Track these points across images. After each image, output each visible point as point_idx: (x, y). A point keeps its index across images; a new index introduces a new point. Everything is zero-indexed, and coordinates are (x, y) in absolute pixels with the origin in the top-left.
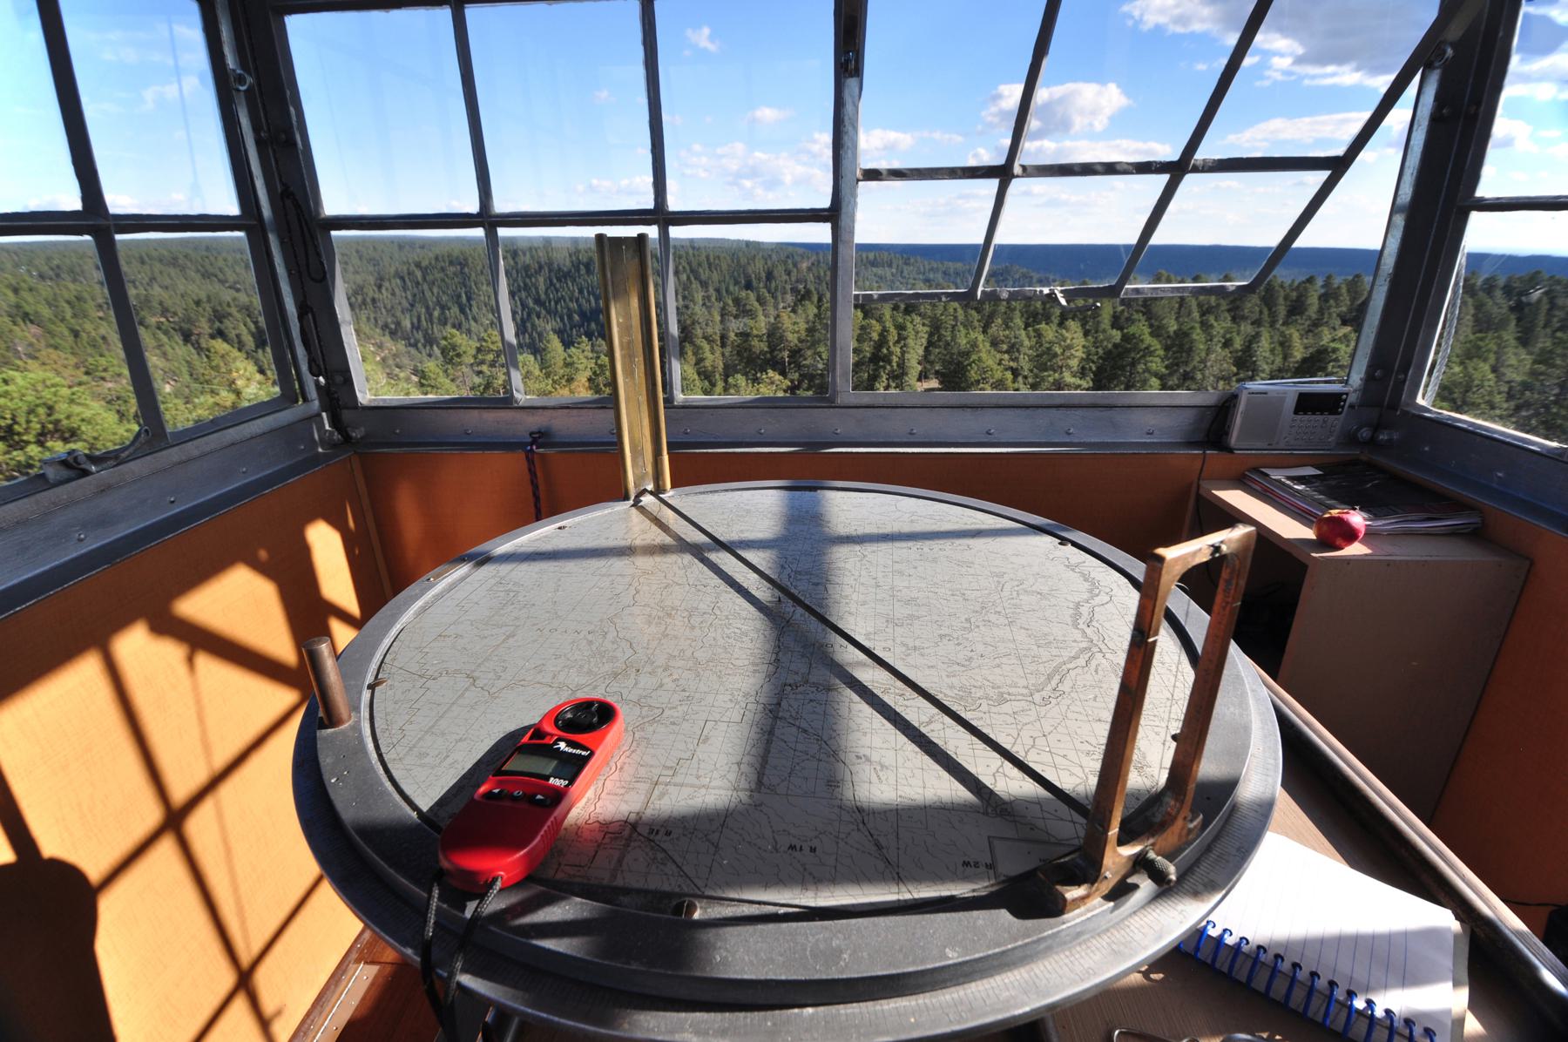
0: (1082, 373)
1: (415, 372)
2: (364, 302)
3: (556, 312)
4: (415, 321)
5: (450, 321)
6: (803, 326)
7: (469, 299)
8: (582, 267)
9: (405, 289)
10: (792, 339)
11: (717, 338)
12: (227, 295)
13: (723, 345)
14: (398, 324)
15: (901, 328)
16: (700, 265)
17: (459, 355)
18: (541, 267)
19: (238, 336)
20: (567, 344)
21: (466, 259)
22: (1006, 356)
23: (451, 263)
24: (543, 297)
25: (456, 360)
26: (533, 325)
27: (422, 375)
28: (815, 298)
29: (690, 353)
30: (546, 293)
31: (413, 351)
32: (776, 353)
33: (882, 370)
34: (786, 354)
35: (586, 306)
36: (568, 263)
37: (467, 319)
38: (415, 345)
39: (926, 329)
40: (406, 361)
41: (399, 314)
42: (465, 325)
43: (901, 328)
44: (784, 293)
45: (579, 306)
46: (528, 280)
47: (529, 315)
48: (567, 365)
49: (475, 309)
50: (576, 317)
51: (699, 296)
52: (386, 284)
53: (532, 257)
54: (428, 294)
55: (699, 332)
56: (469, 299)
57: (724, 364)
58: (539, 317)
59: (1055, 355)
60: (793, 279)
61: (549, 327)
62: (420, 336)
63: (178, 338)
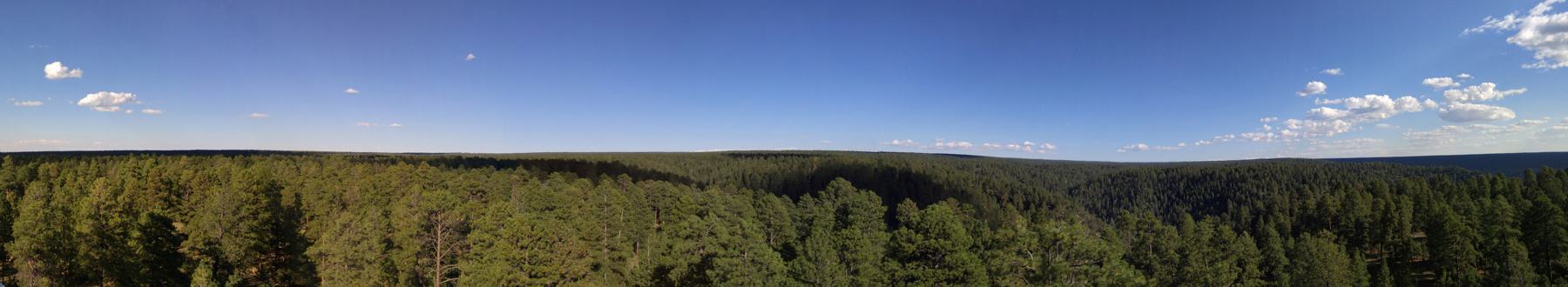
0: (1514, 225)
1: (1099, 231)
2: (1079, 193)
3: (1189, 202)
4: (1104, 204)
5: (1123, 206)
6: (1339, 203)
7: (1135, 194)
8: (1208, 177)
9: (1101, 187)
10: (1333, 210)
11: (1287, 211)
12: (1018, 184)
13: (1291, 215)
14: (1094, 205)
15: (1397, 202)
16: (1276, 172)
17: (1127, 224)
18: (1182, 178)
19: (1018, 203)
20: (1197, 219)
21: (1137, 174)
22: (1464, 217)
23: (1128, 176)
24: (1182, 192)
25: (1125, 226)
26: (1174, 211)
27: (1104, 234)
28: (1343, 187)
29: (1272, 221)
30: (1184, 191)
31: (1100, 220)
32: (1323, 218)
33: (1388, 227)
34: (1330, 219)
35: (1208, 196)
36: (1200, 174)
37: (1133, 205)
38: (1101, 217)
39: (1412, 203)
40: (1095, 225)
41: (1095, 199)
42: (1131, 208)
43: (1397, 202)
44: (1324, 185)
45: (1204, 197)
46: (1173, 185)
47: (1172, 204)
48: (1196, 231)
49: (1138, 200)
50: (1202, 204)
51: (1276, 189)
52: (1092, 185)
53: (1177, 172)
54: (1113, 191)
55: (1277, 208)
56: (1135, 194)
57: (1292, 225)
58: (1178, 204)
59: (1497, 215)
60: (1329, 177)
61: (1184, 211)
62: (1104, 212)
63: (995, 200)
